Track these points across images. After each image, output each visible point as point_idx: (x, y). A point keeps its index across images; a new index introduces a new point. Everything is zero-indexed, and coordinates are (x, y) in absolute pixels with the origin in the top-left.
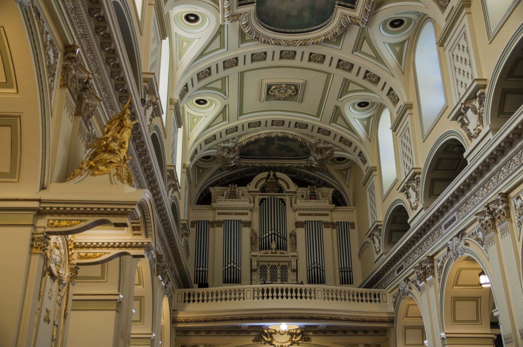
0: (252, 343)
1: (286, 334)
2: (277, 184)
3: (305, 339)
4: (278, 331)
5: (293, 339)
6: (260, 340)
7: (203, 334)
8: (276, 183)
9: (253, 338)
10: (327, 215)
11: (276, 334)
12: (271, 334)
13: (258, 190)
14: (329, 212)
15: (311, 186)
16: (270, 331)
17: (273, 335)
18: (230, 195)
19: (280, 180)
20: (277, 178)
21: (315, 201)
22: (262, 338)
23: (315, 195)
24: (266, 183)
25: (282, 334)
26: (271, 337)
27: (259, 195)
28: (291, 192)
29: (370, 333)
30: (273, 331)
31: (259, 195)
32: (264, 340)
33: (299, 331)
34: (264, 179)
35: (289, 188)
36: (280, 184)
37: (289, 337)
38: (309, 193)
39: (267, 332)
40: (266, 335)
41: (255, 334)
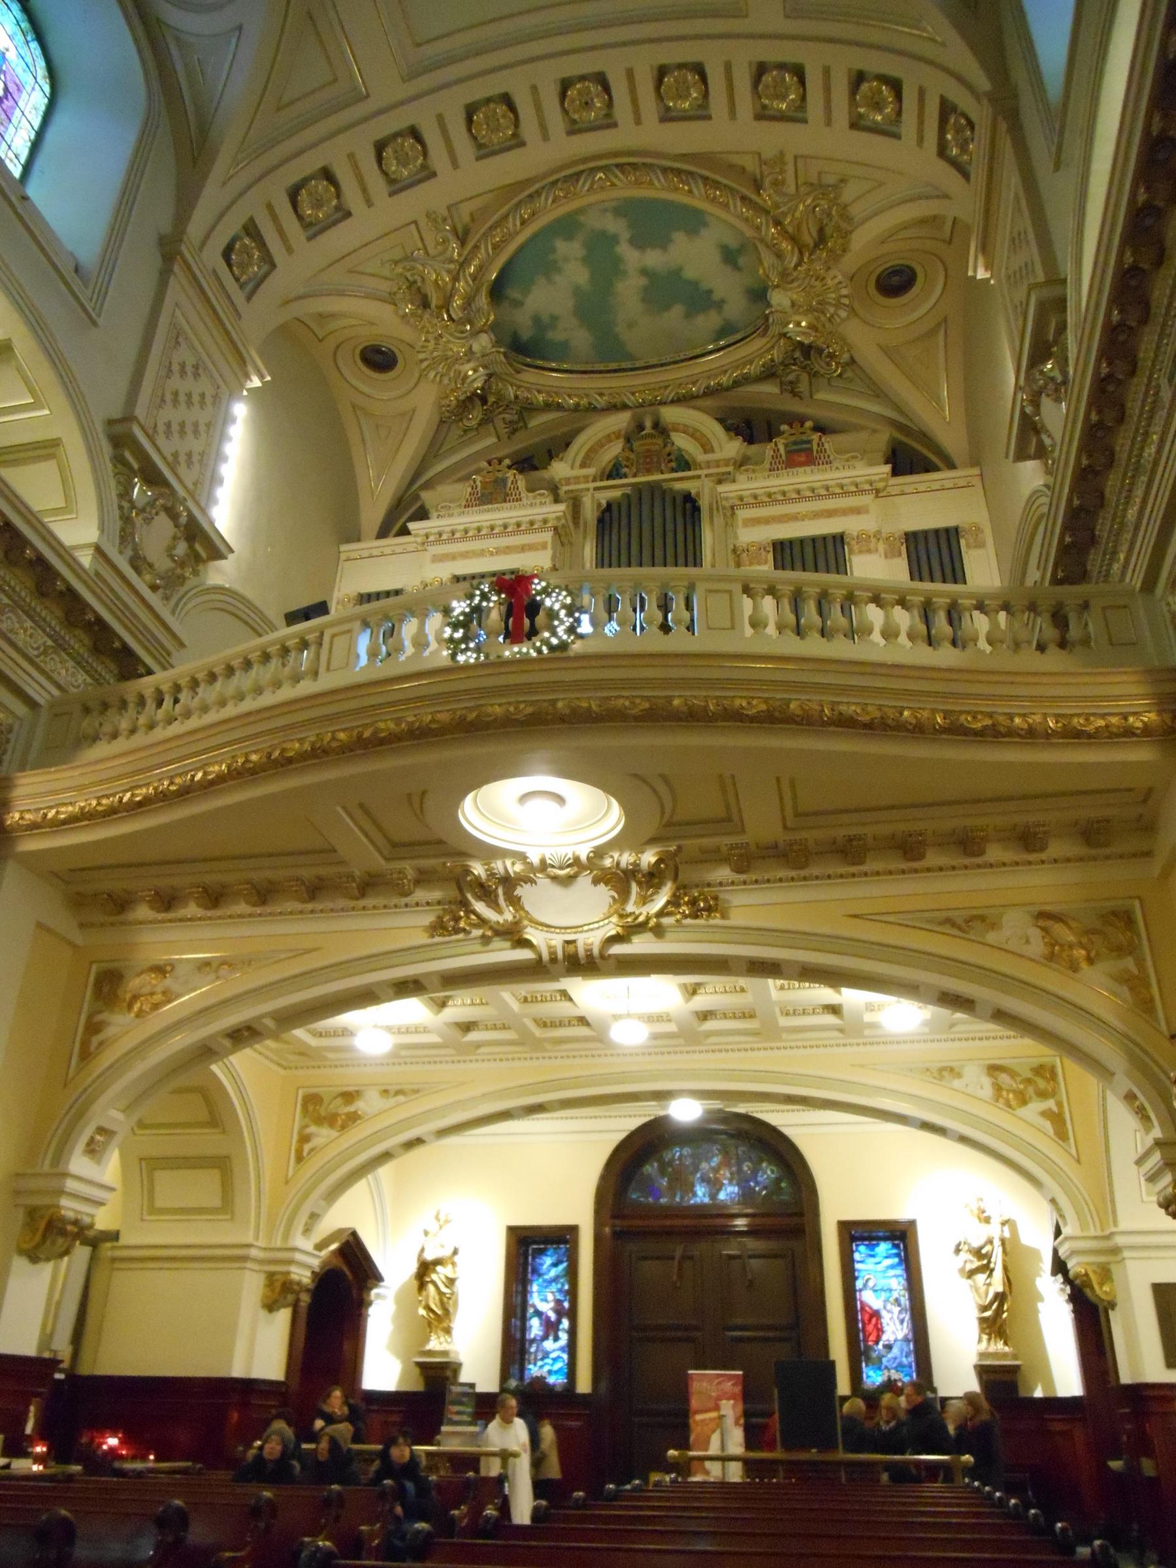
0: (423, 939)
1: (585, 880)
2: (668, 449)
3: (693, 903)
4: (535, 859)
5: (630, 908)
6: (462, 924)
7: (192, 909)
8: (665, 446)
9: (428, 919)
10: (857, 511)
11: (533, 882)
12: (509, 882)
13: (591, 471)
14: (867, 500)
15: (791, 425)
16: (499, 866)
17: (519, 891)
18: (482, 495)
19: (676, 430)
20: (661, 429)
21: (808, 469)
22: (470, 911)
23: (811, 450)
24: (628, 454)
25: (567, 881)
26: (515, 902)
27: (596, 489)
28: (717, 464)
29: (1056, 849)
30: (518, 867)
31: (596, 489)
32: (483, 922)
33: (649, 858)
34: (618, 437)
35: (707, 448)
36: (679, 449)
37: (604, 894)
38: (786, 445)
39: (484, 876)
40: (485, 892)
41: (437, 895)
